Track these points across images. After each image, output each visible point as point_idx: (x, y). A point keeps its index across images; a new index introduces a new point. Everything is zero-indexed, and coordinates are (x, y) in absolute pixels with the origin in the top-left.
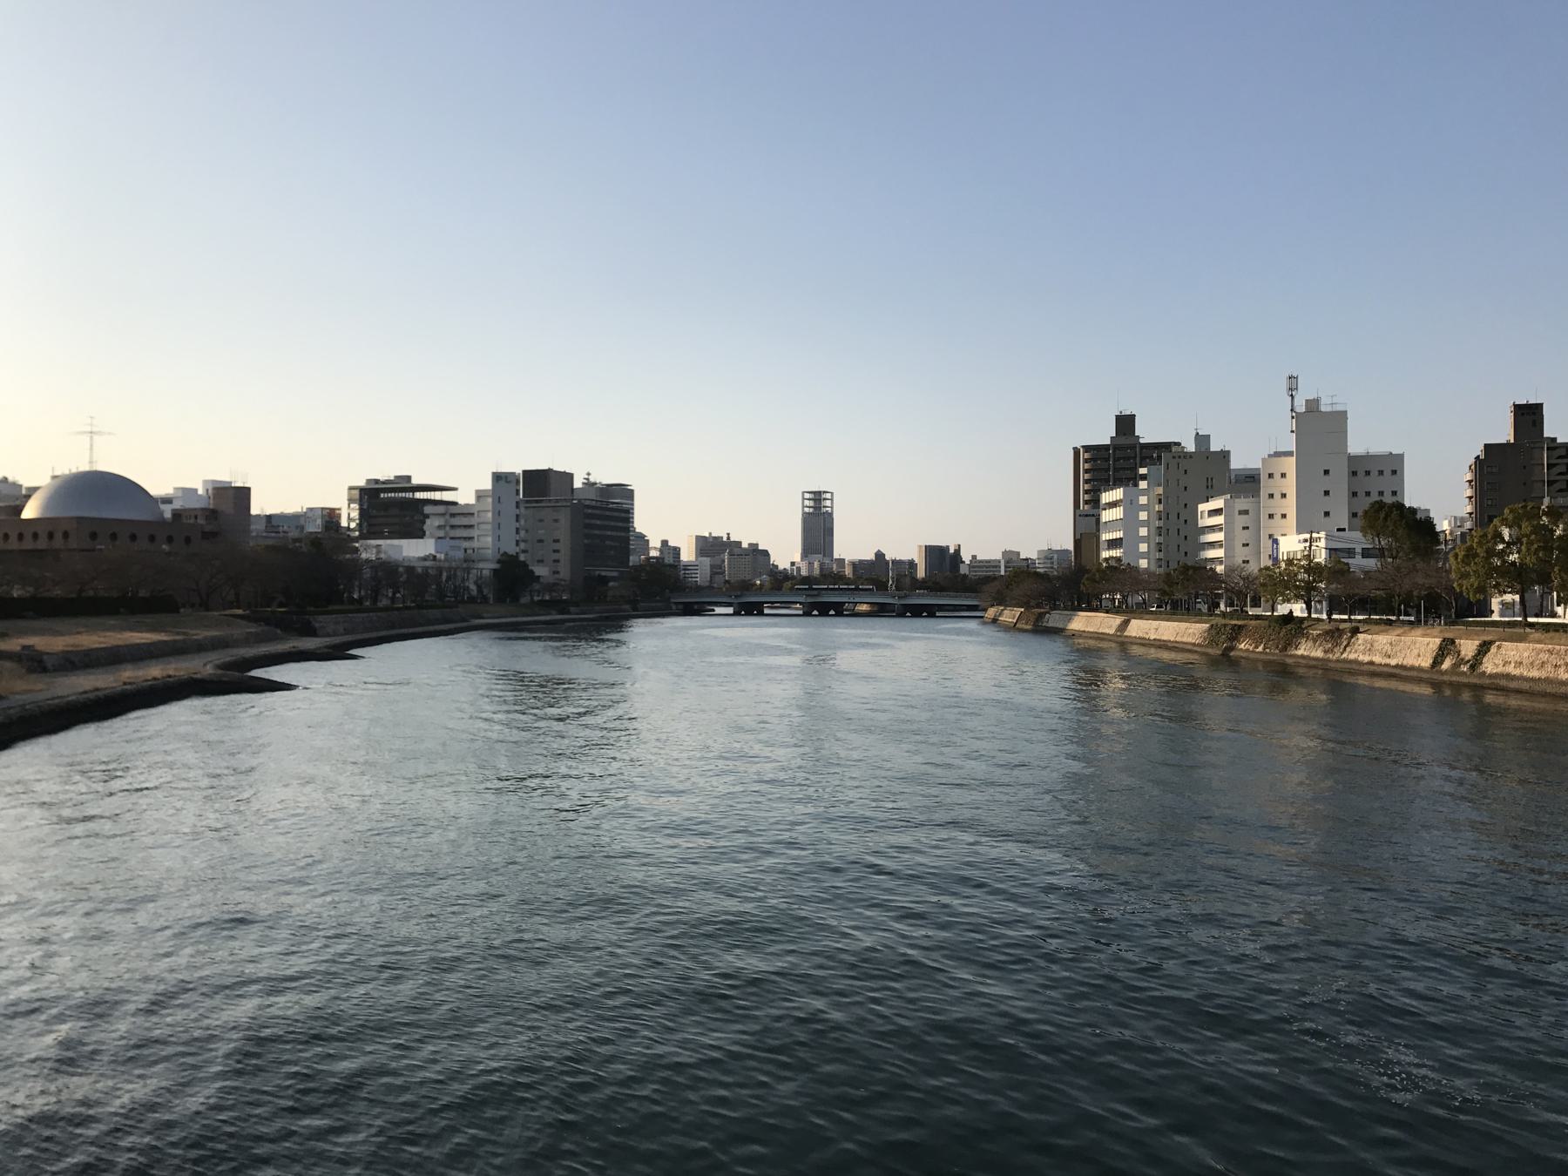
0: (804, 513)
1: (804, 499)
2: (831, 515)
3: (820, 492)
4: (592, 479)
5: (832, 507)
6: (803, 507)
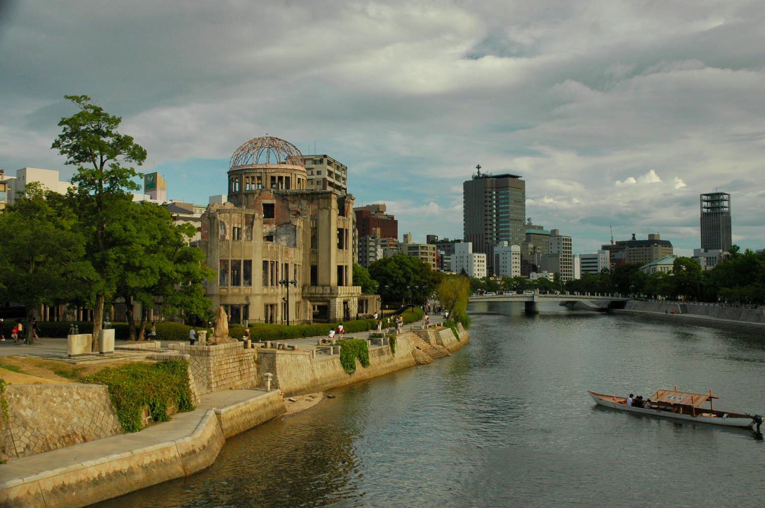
0: (703, 214)
1: (702, 201)
2: (728, 213)
3: (718, 194)
4: (483, 171)
5: (729, 207)
6: (702, 208)
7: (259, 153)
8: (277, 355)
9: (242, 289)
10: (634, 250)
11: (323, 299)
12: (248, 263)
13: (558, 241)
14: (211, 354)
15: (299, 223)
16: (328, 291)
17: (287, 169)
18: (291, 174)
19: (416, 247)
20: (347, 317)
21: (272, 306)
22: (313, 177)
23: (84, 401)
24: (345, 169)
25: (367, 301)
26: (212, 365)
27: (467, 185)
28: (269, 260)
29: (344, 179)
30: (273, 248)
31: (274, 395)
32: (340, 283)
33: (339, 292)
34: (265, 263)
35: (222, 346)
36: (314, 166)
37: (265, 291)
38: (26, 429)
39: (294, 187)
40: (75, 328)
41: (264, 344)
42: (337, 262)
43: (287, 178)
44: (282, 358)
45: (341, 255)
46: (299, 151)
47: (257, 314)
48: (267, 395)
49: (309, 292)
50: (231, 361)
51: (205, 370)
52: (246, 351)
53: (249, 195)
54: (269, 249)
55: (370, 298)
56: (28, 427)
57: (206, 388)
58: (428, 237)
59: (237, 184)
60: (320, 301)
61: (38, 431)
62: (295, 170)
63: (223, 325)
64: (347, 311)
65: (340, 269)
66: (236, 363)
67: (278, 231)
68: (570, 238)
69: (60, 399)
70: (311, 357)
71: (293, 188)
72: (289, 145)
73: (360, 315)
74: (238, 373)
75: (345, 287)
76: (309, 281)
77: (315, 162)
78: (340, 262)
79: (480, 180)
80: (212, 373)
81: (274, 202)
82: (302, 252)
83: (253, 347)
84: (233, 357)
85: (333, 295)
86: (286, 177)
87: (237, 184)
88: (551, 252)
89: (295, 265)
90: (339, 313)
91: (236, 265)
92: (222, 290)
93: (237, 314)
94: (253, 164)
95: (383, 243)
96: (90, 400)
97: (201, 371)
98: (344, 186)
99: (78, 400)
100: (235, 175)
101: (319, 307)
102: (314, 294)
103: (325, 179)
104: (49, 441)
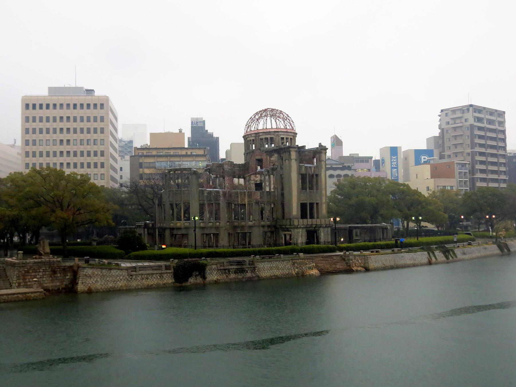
16: (289, 224)
17: (270, 132)
24: (502, 114)
46: (290, 118)
49: (280, 224)
53: (249, 154)
59: (254, 145)
63: (44, 249)
72: (284, 114)
76: (280, 215)
78: (303, 200)
87: (254, 145)
94: (277, 128)
98: (501, 129)
103: (471, 125)
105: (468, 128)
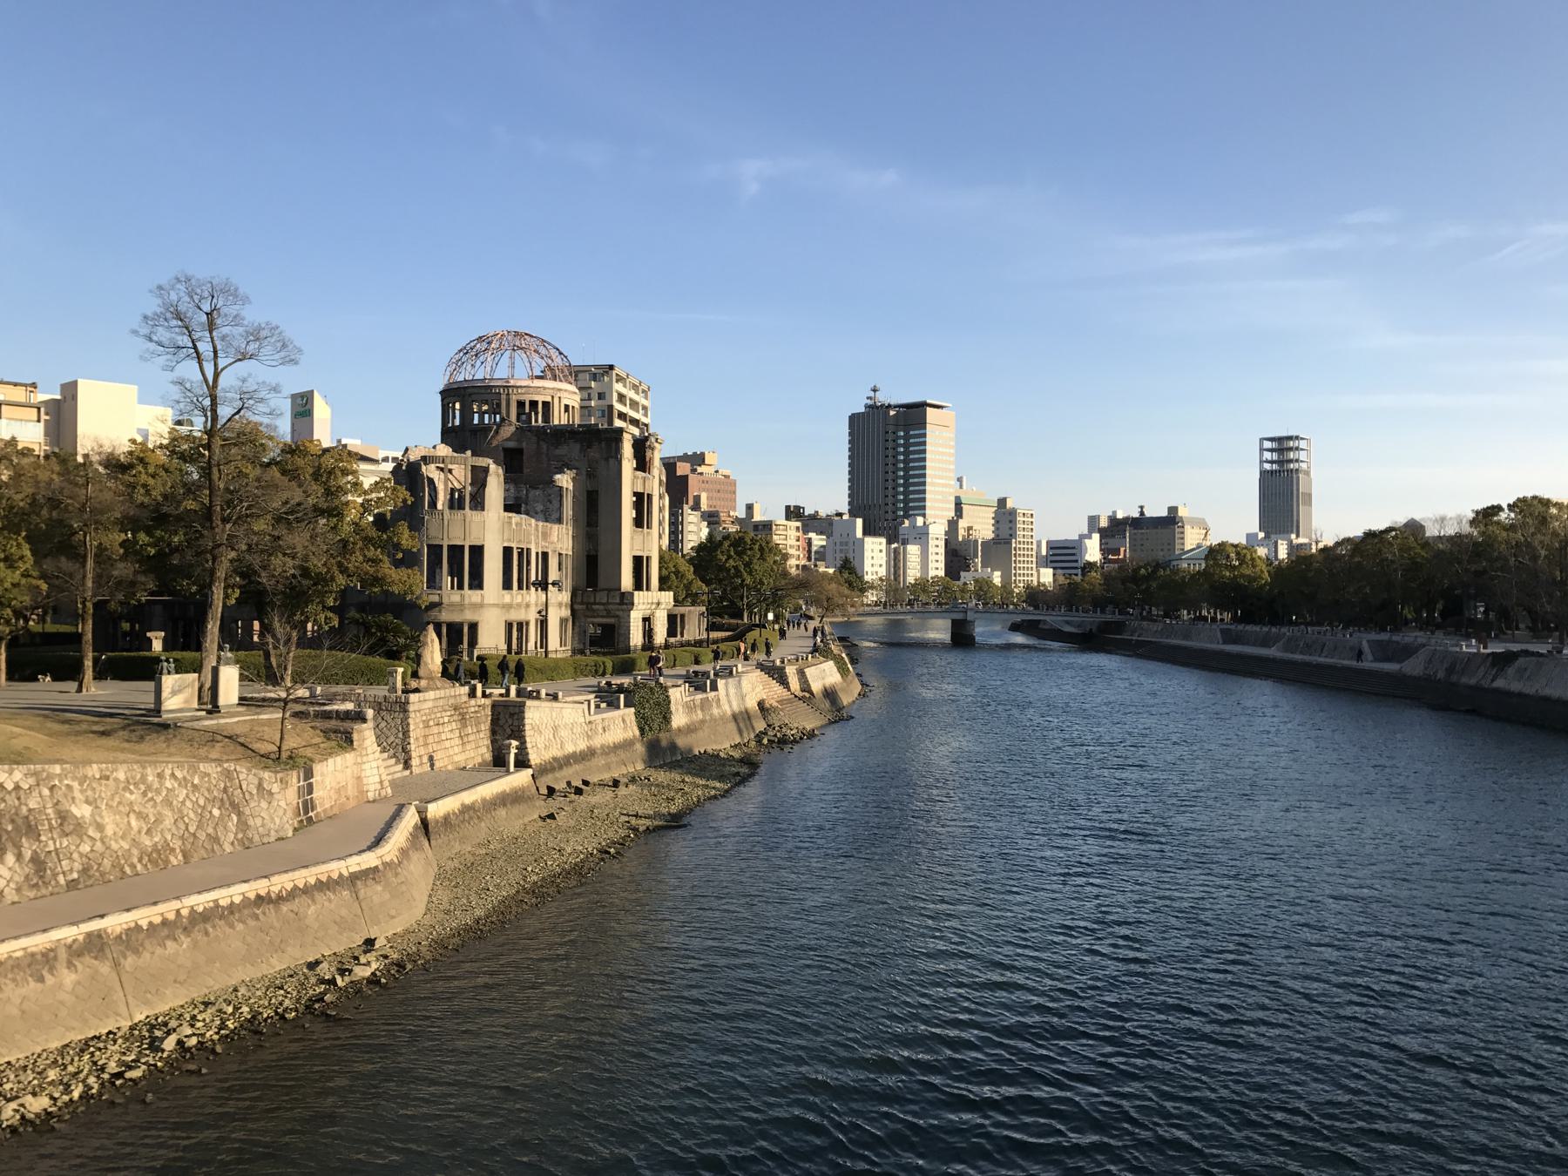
1: (1262, 450)
4: (883, 398)
7: (497, 359)
8: (527, 710)
9: (466, 596)
10: (1142, 533)
11: (609, 614)
12: (477, 552)
13: (1010, 518)
14: (411, 708)
15: (565, 480)
16: (618, 601)
17: (545, 388)
18: (553, 397)
19: (767, 526)
20: (648, 644)
21: (520, 625)
22: (593, 404)
23: (185, 791)
25: (683, 616)
26: (412, 727)
27: (854, 419)
28: (514, 545)
29: (645, 408)
30: (521, 524)
31: (522, 778)
32: (638, 585)
33: (636, 601)
34: (507, 552)
35: (431, 694)
36: (593, 383)
37: (507, 597)
38: (82, 841)
39: (559, 418)
40: (169, 662)
41: (503, 691)
42: (632, 549)
43: (546, 405)
44: (537, 715)
45: (638, 538)
47: (491, 641)
48: (509, 778)
50: (446, 720)
51: (400, 735)
52: (473, 702)
54: (514, 526)
55: (689, 611)
56: (85, 838)
57: (401, 766)
58: (788, 508)
60: (602, 617)
61: (103, 843)
62: (560, 390)
63: (432, 658)
64: (648, 633)
65: (638, 562)
66: (454, 724)
67: (530, 495)
68: (1030, 512)
69: (143, 787)
70: (586, 711)
71: (556, 422)
73: (672, 640)
74: (458, 741)
75: (645, 593)
77: (594, 377)
79: (876, 411)
80: (412, 741)
81: (524, 445)
82: (571, 533)
83: (484, 695)
84: (449, 713)
85: (626, 601)
86: (544, 403)
88: (998, 536)
89: (560, 554)
90: (636, 638)
91: (456, 551)
92: (431, 596)
93: (458, 636)
95: (711, 519)
96: (195, 787)
97: (392, 739)
99: (173, 790)
100: (451, 394)
101: (604, 626)
102: (592, 604)
103: (611, 407)
104: (123, 862)
105: (603, 411)
